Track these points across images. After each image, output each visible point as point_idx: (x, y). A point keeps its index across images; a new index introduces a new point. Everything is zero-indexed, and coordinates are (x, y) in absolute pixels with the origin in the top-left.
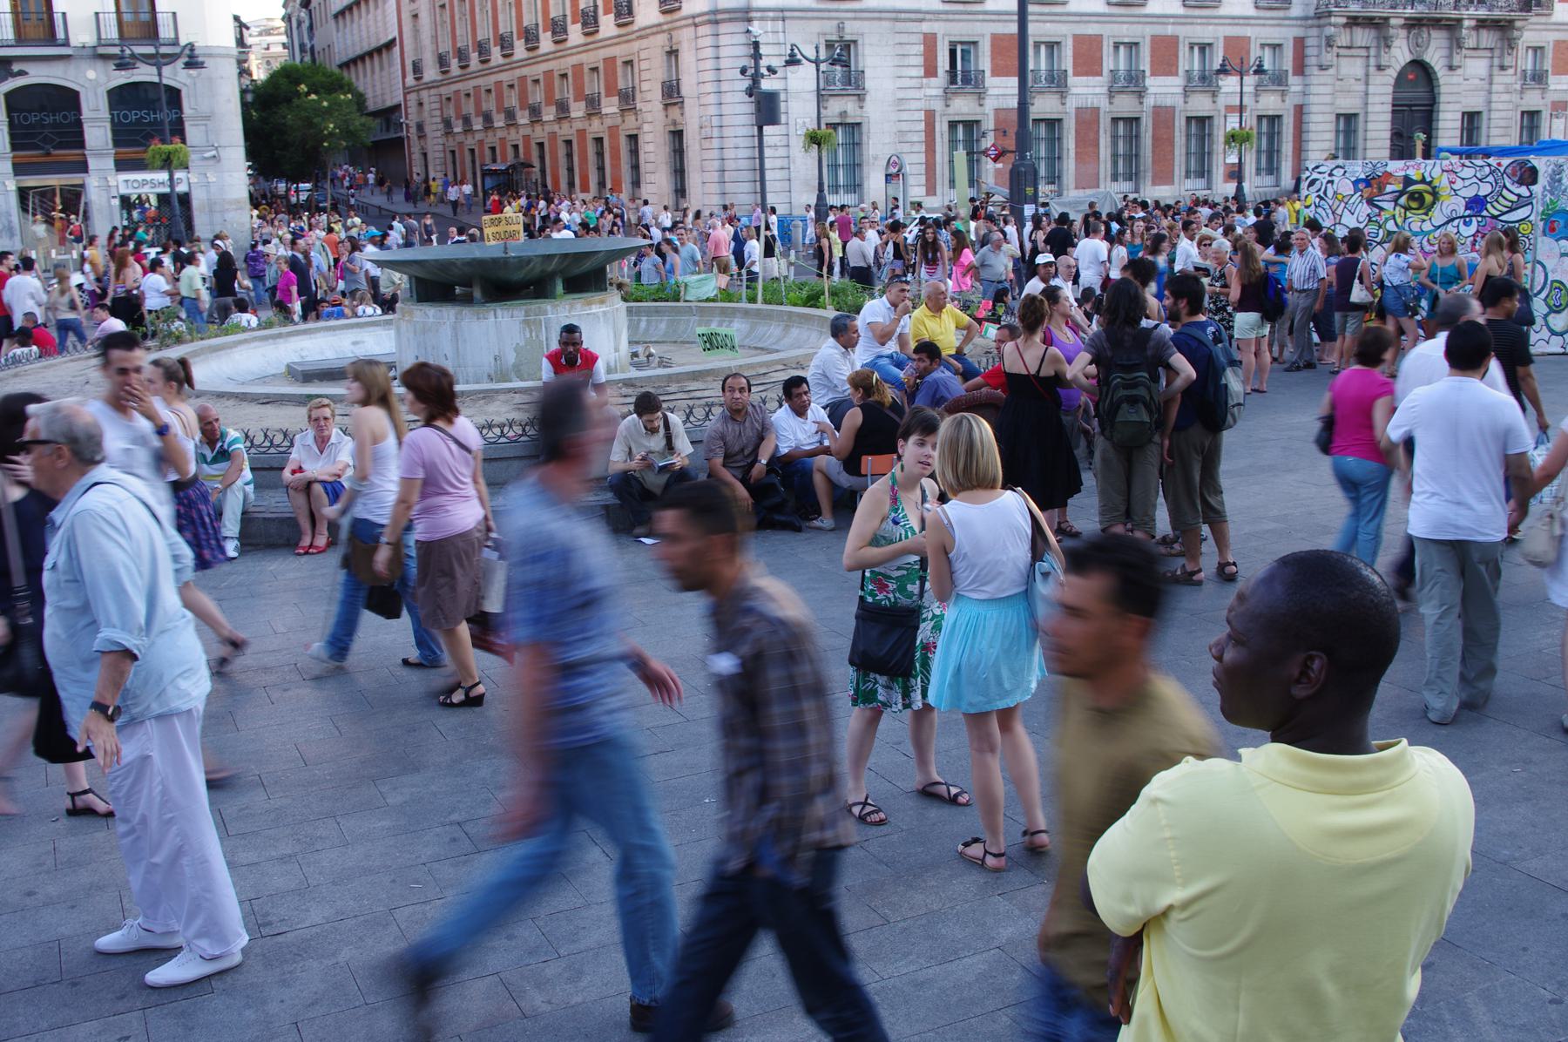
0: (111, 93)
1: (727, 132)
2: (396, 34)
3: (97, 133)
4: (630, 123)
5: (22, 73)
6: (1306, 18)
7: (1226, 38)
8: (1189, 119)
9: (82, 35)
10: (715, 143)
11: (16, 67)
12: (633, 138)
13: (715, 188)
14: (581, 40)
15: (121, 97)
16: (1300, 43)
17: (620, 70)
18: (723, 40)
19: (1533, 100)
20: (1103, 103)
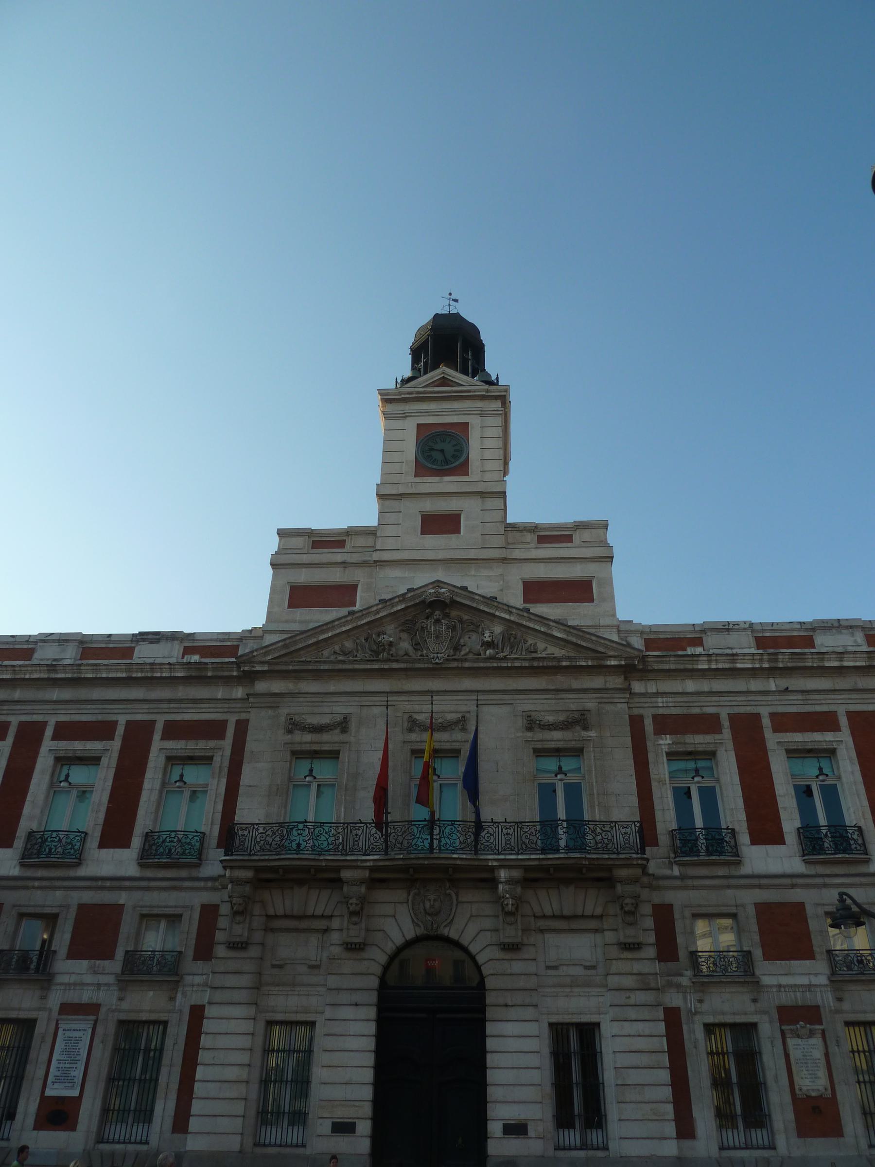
7: (81, 907)
16: (209, 913)
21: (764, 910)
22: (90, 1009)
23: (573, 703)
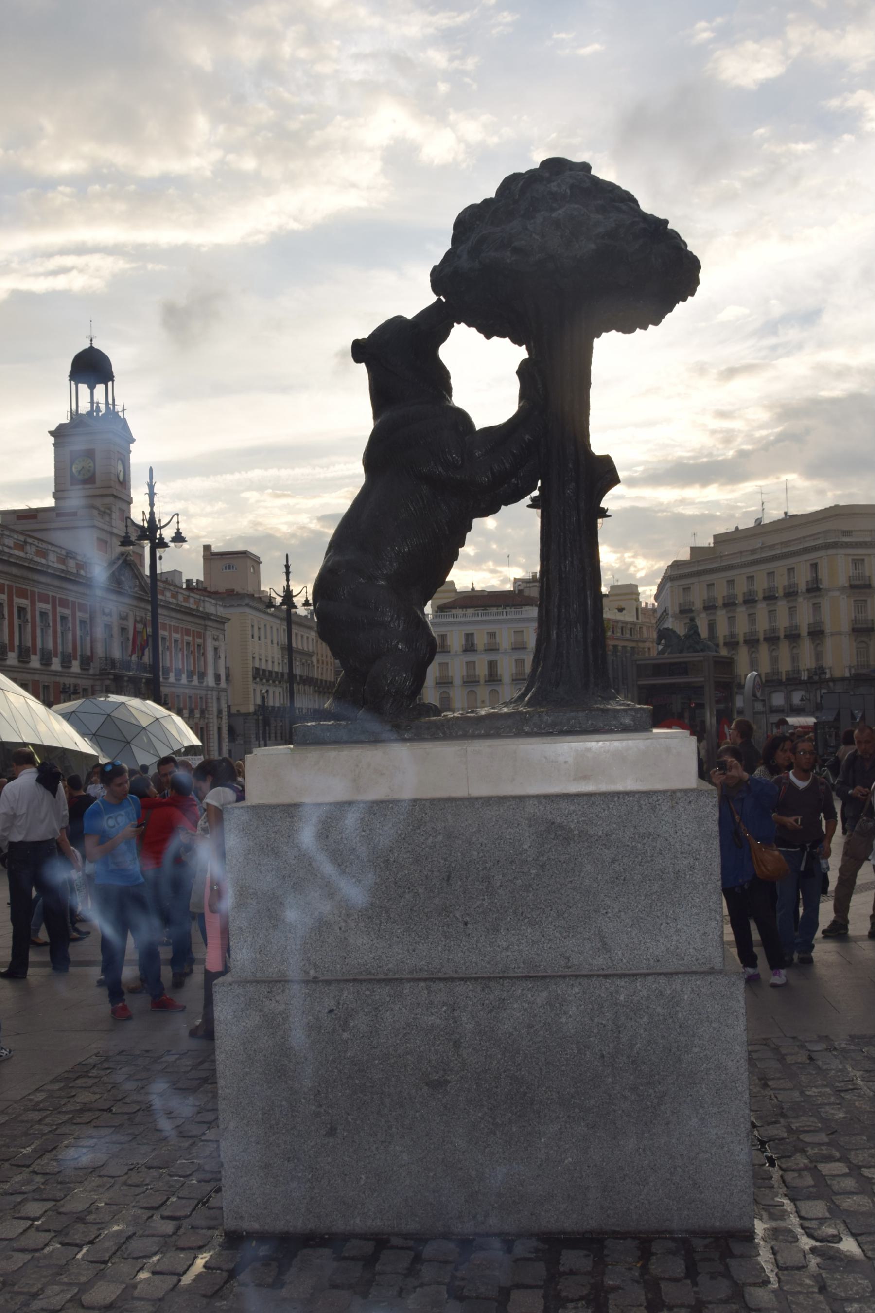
6: (94, 675)
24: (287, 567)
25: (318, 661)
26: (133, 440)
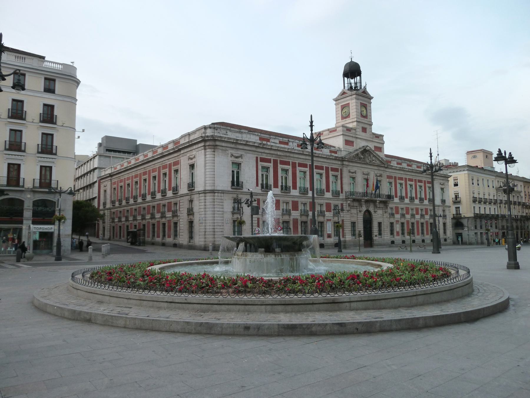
0: (34, 202)
1: (207, 222)
2: (97, 195)
3: (28, 214)
4: (175, 219)
5: (7, 194)
7: (326, 203)
8: (319, 222)
9: (29, 185)
10: (203, 224)
11: (5, 193)
12: (176, 224)
13: (203, 236)
14: (161, 197)
15: (36, 203)
16: (342, 205)
17: (173, 205)
18: (207, 198)
19: (392, 220)
20: (299, 218)
21: (396, 207)
22: (330, 220)
23: (382, 172)
24: (312, 122)
25: (525, 195)
26: (372, 98)
